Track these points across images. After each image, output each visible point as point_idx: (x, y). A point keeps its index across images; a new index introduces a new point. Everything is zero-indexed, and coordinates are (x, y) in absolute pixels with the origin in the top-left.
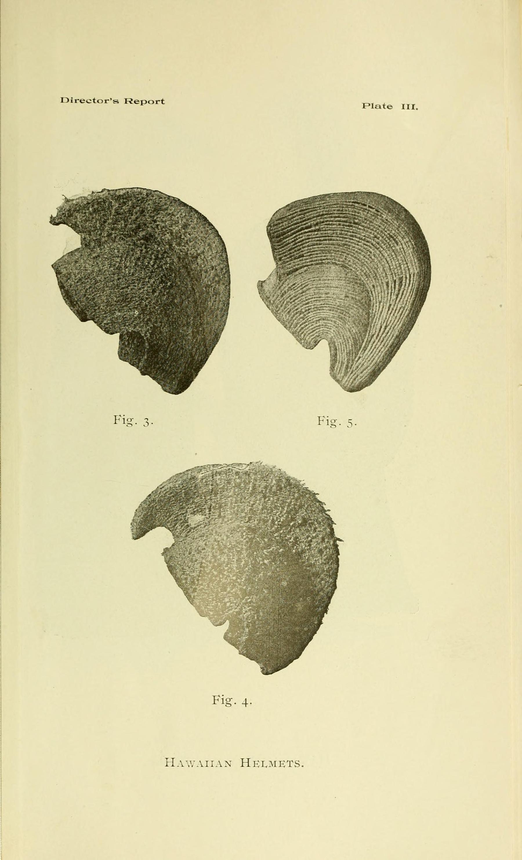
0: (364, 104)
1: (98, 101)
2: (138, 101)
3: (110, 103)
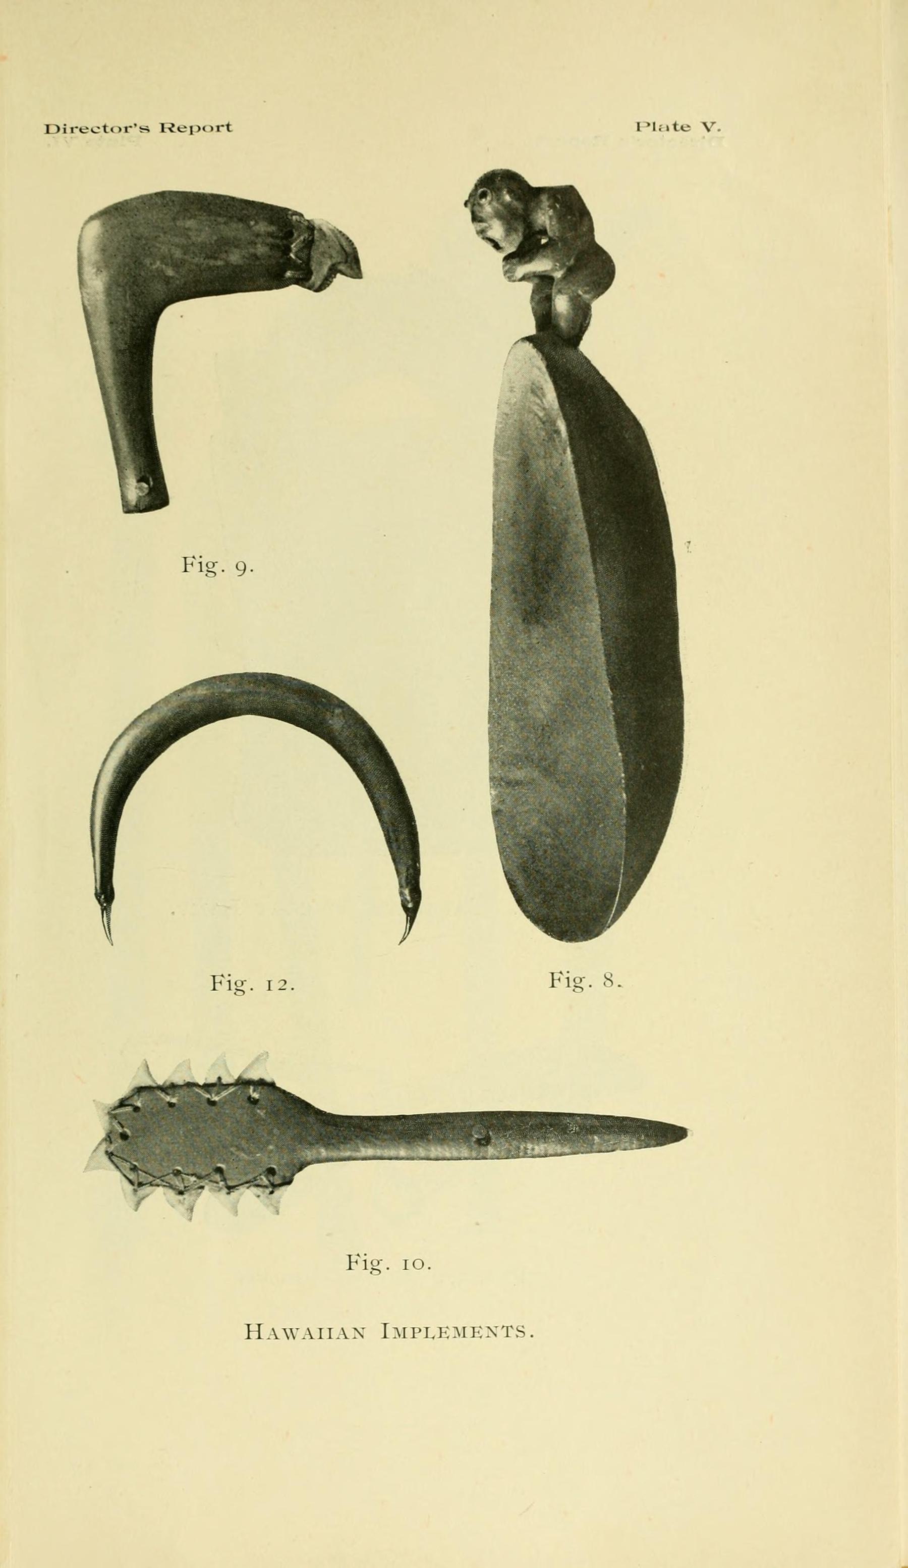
0: (638, 124)
1: (112, 130)
2: (185, 127)
3: (134, 131)
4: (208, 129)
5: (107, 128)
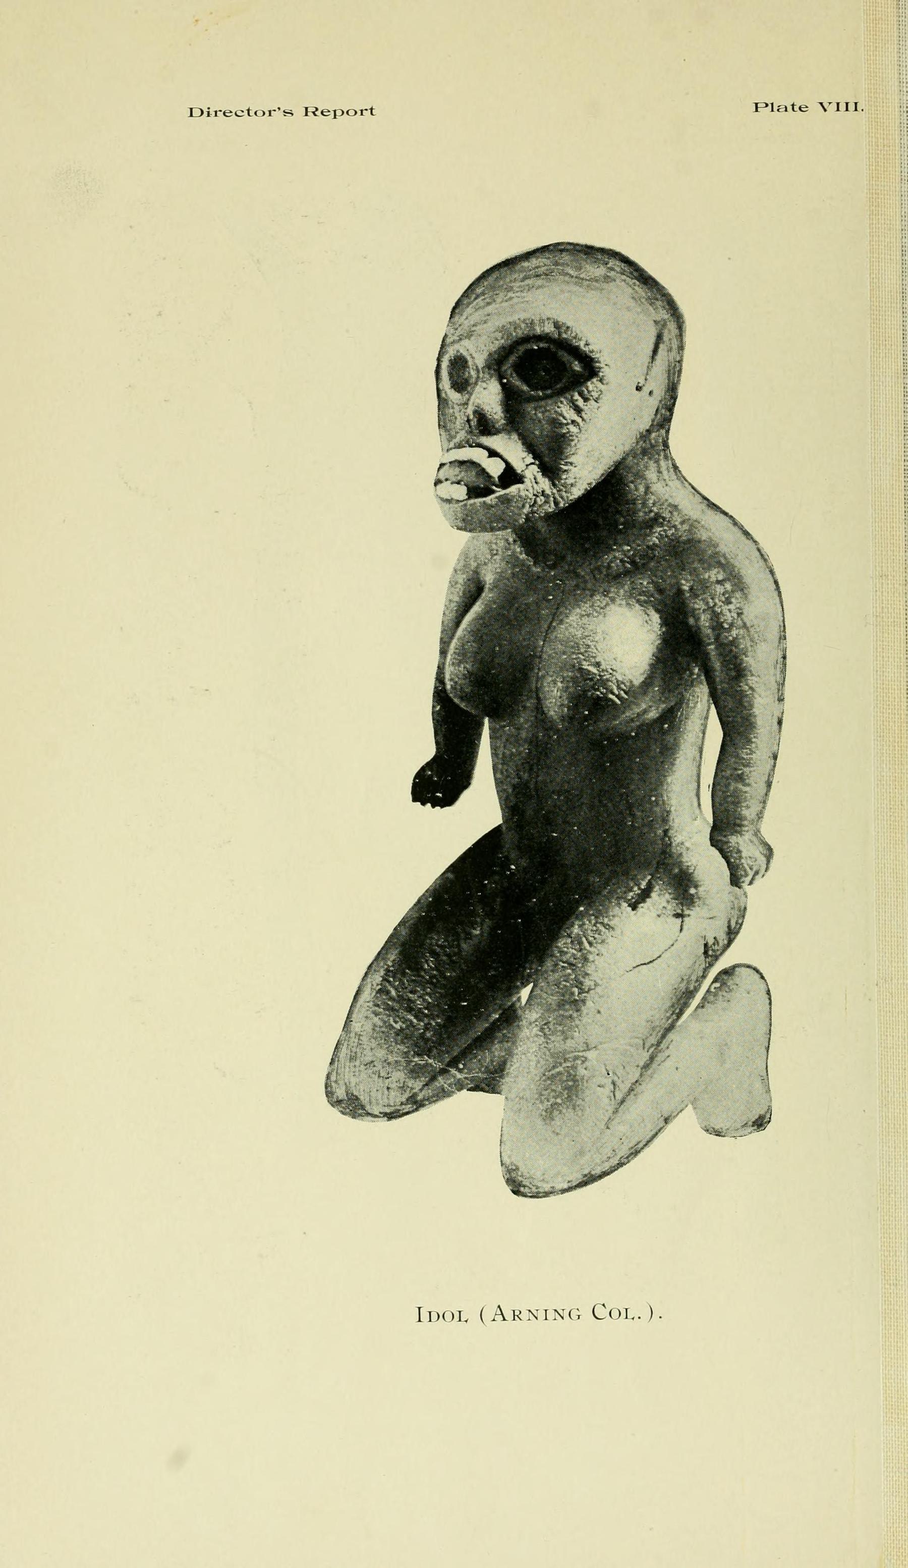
0: (756, 104)
1: (256, 113)
2: (329, 111)
4: (352, 113)
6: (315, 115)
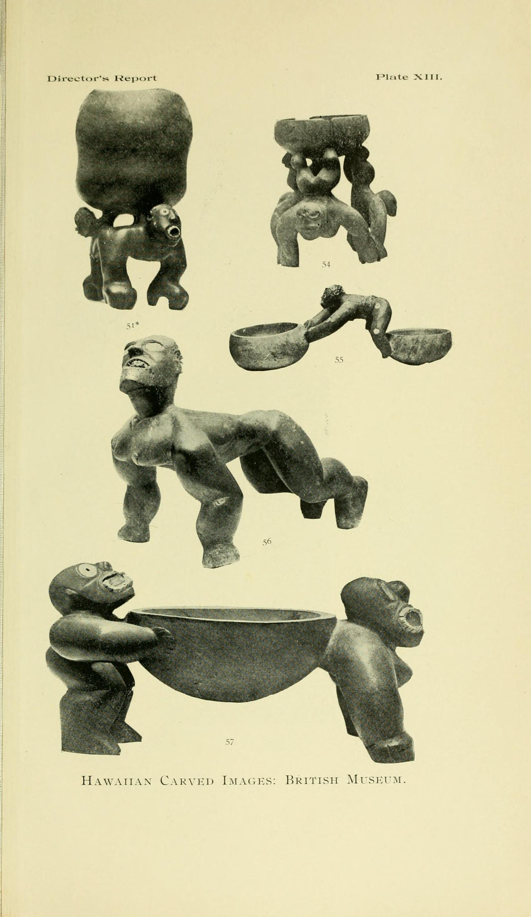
0: (378, 75)
1: (87, 79)
2: (129, 78)
4: (143, 79)
5: (84, 78)
6: (121, 80)
